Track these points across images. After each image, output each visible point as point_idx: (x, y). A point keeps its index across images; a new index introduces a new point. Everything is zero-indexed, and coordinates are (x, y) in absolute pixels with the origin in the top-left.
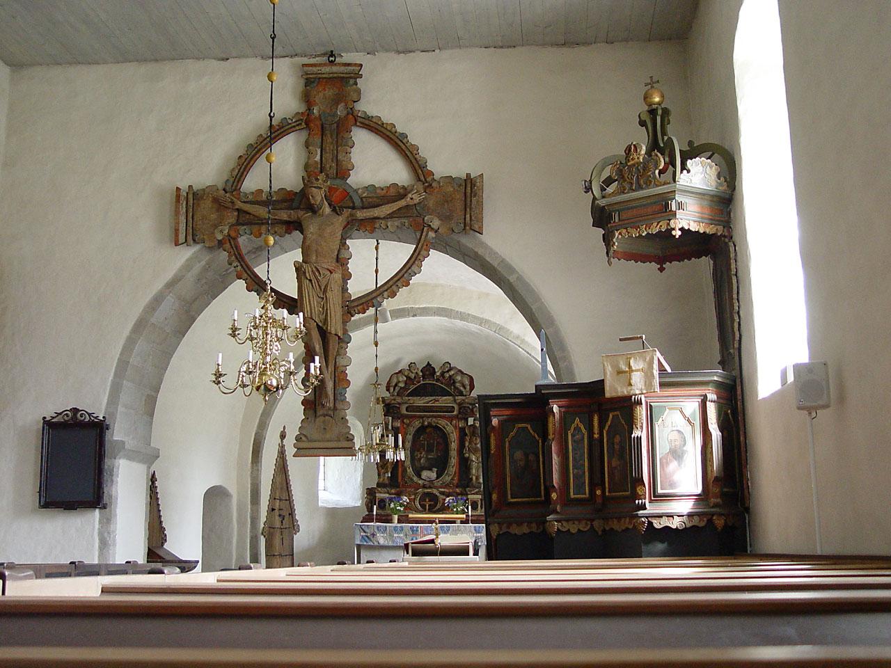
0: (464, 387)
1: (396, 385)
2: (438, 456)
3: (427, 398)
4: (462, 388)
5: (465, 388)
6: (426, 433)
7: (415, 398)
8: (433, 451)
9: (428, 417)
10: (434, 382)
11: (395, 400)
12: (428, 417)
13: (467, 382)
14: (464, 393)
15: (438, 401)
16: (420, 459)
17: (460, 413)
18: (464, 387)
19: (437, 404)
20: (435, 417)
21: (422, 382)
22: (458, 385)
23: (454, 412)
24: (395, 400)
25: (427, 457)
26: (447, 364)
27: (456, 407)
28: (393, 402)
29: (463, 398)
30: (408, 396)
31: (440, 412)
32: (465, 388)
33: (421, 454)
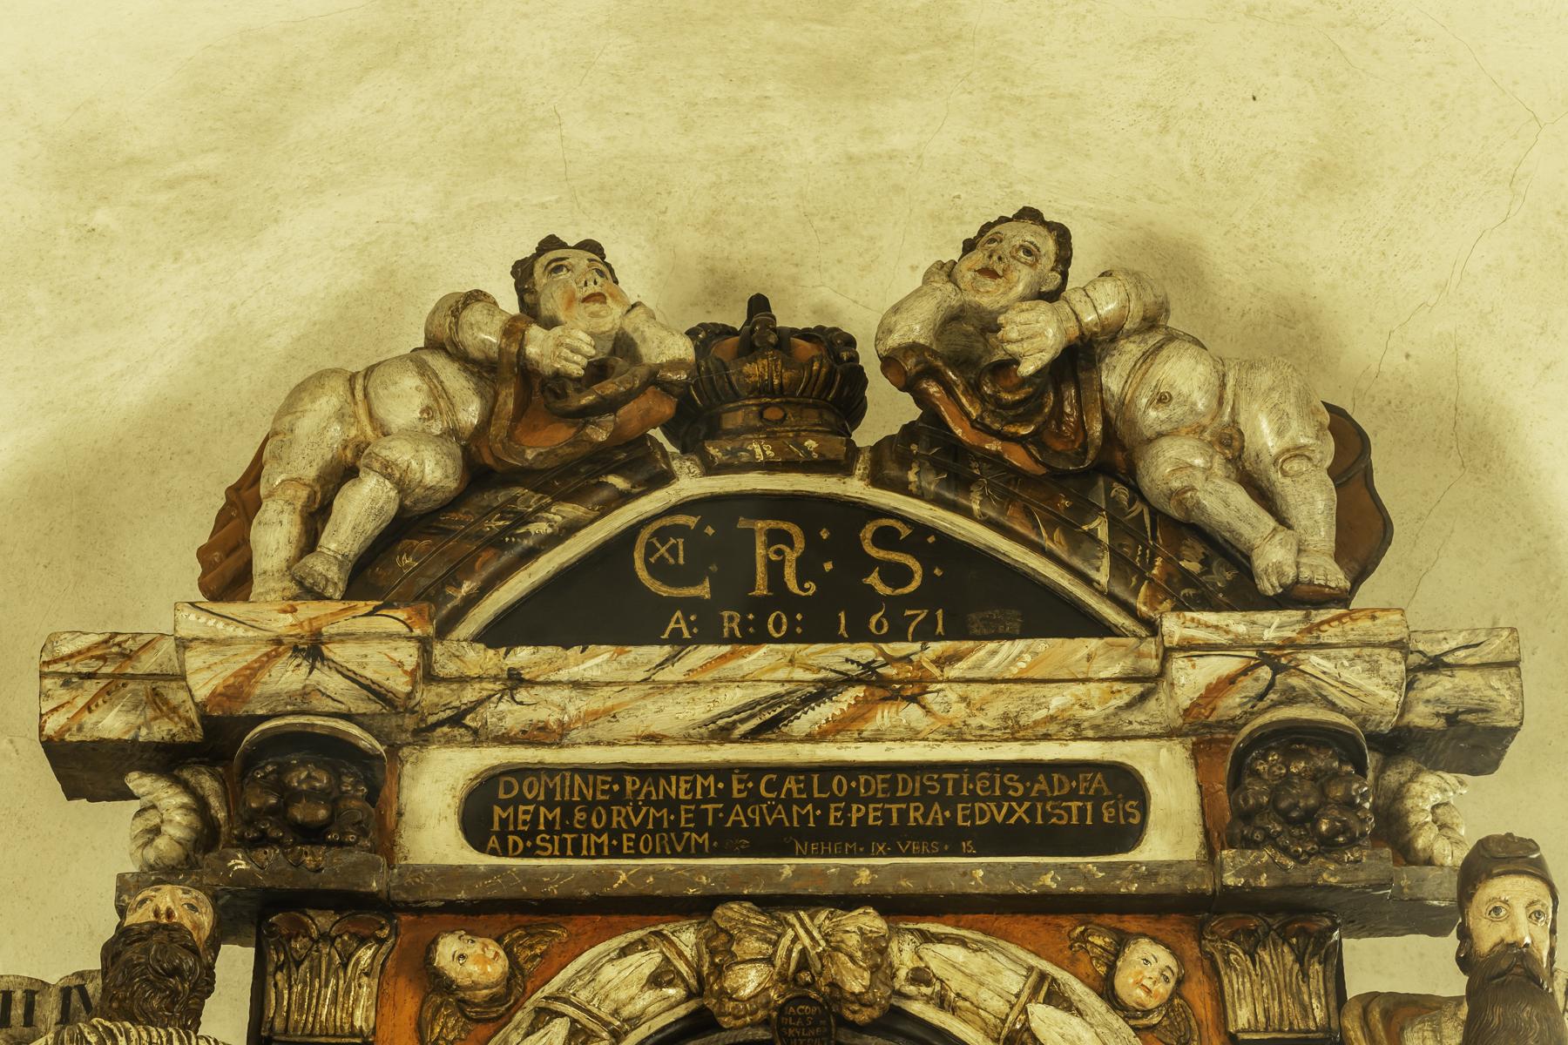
1: (342, 473)
3: (760, 658)
7: (597, 662)
9: (776, 903)
10: (855, 487)
11: (312, 649)
12: (776, 903)
20: (896, 906)
21: (690, 483)
23: (1130, 836)
24: (312, 649)
26: (1027, 233)
28: (288, 676)
29: (1273, 626)
30: (499, 634)
31: (949, 840)
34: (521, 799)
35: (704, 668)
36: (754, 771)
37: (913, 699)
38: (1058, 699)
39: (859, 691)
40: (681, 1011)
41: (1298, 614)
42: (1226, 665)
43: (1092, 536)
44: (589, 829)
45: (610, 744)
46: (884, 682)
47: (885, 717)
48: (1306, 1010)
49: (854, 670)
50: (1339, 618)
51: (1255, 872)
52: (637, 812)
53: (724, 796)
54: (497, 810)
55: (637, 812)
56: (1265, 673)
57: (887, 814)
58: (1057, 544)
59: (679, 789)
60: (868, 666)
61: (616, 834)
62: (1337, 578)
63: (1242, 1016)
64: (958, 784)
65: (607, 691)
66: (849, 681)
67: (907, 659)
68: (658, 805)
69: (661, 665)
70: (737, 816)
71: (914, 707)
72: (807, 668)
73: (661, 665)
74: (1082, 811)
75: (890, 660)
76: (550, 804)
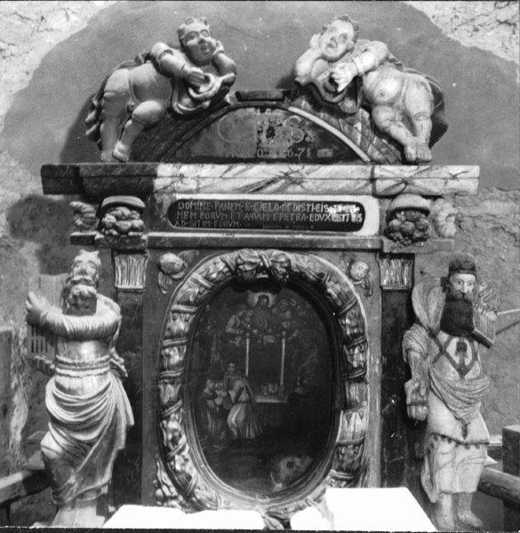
0: (408, 120)
2: (294, 398)
4: (400, 132)
5: (412, 128)
6: (249, 307)
8: (276, 381)
13: (419, 102)
14: (411, 152)
15: (294, 182)
16: (224, 413)
17: (387, 231)
18: (408, 120)
19: (293, 196)
22: (384, 116)
23: (357, 226)
25: (249, 402)
27: (373, 208)
29: (407, 171)
32: (412, 128)
33: (229, 387)
34: (184, 210)
35: (238, 173)
36: (252, 202)
37: (299, 184)
38: (342, 185)
39: (283, 181)
40: (230, 278)
41: (416, 167)
42: (392, 183)
43: (356, 128)
44: (205, 220)
45: (211, 193)
46: (290, 179)
47: (290, 189)
48: (402, 281)
49: (282, 175)
50: (427, 169)
51: (393, 248)
52: (218, 213)
53: (244, 209)
54: (178, 213)
55: (218, 213)
56: (404, 185)
57: (290, 216)
58: (346, 129)
59: (230, 207)
60: (287, 174)
61: (213, 221)
62: (428, 155)
63: (384, 282)
64: (311, 208)
65: (208, 180)
66: (281, 178)
67: (298, 172)
68: (224, 212)
69: (225, 172)
70: (247, 216)
71: (299, 187)
72: (269, 174)
73: (225, 172)
74: (346, 217)
75: (293, 172)
76: (194, 211)
